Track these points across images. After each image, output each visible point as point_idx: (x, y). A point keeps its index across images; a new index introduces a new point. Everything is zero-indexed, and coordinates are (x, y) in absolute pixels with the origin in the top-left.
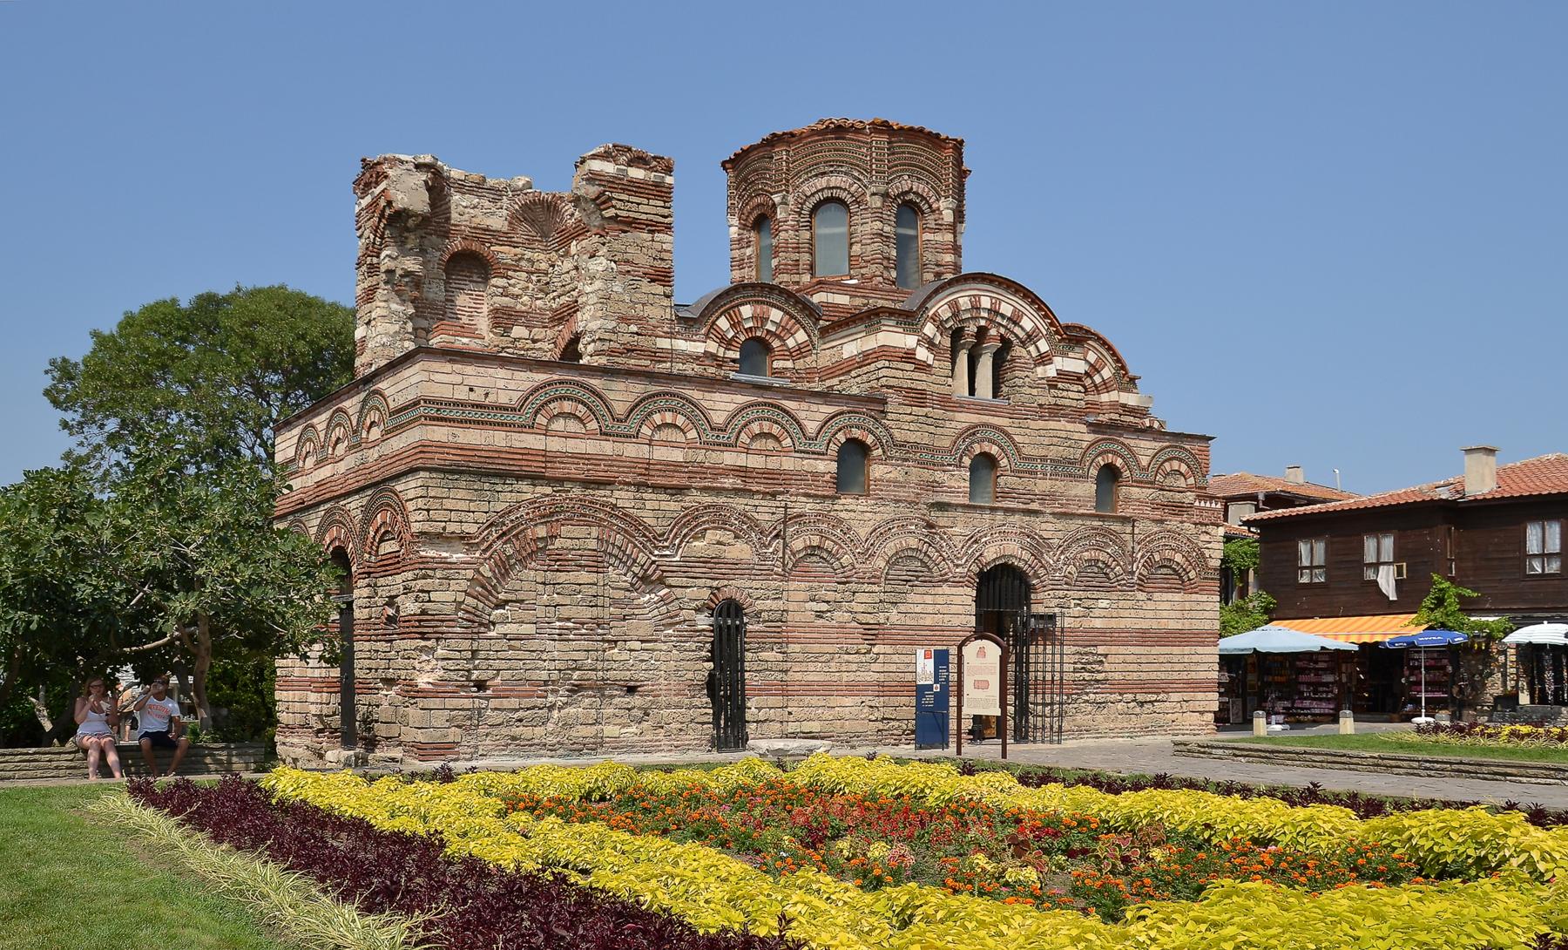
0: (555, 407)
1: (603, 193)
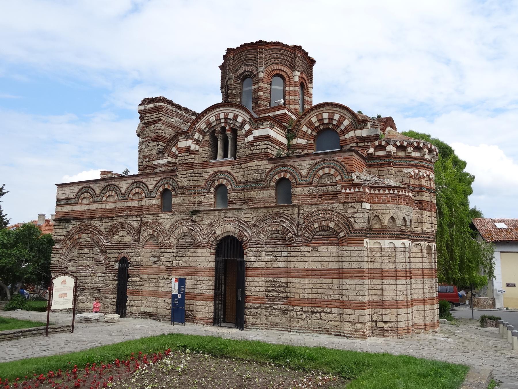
0: (83, 196)
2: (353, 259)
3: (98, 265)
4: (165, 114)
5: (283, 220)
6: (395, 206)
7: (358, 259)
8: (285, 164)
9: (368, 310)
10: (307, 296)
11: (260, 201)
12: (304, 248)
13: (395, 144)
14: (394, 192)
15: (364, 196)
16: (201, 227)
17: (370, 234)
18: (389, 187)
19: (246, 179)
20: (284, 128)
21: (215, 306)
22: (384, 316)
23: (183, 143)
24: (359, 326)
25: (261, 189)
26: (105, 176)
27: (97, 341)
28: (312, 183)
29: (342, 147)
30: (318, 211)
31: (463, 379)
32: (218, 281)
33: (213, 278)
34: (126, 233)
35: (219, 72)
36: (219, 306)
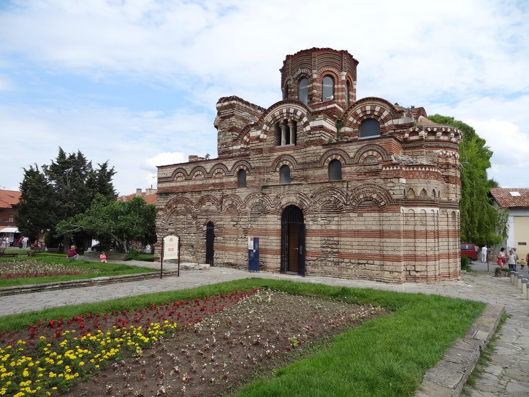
0: (177, 175)
2: (392, 223)
4: (237, 110)
5: (335, 192)
6: (426, 180)
7: (395, 223)
8: (337, 149)
9: (403, 262)
10: (354, 251)
11: (316, 178)
12: (351, 214)
13: (426, 130)
14: (425, 169)
15: (401, 173)
16: (270, 198)
17: (406, 203)
18: (422, 166)
19: (304, 161)
20: (334, 119)
21: (281, 258)
22: (416, 267)
23: (254, 133)
24: (396, 274)
25: (317, 169)
26: (192, 159)
27: (199, 283)
28: (358, 163)
29: (382, 133)
30: (363, 185)
31: (481, 311)
32: (283, 240)
33: (280, 238)
35: (280, 74)
36: (284, 259)
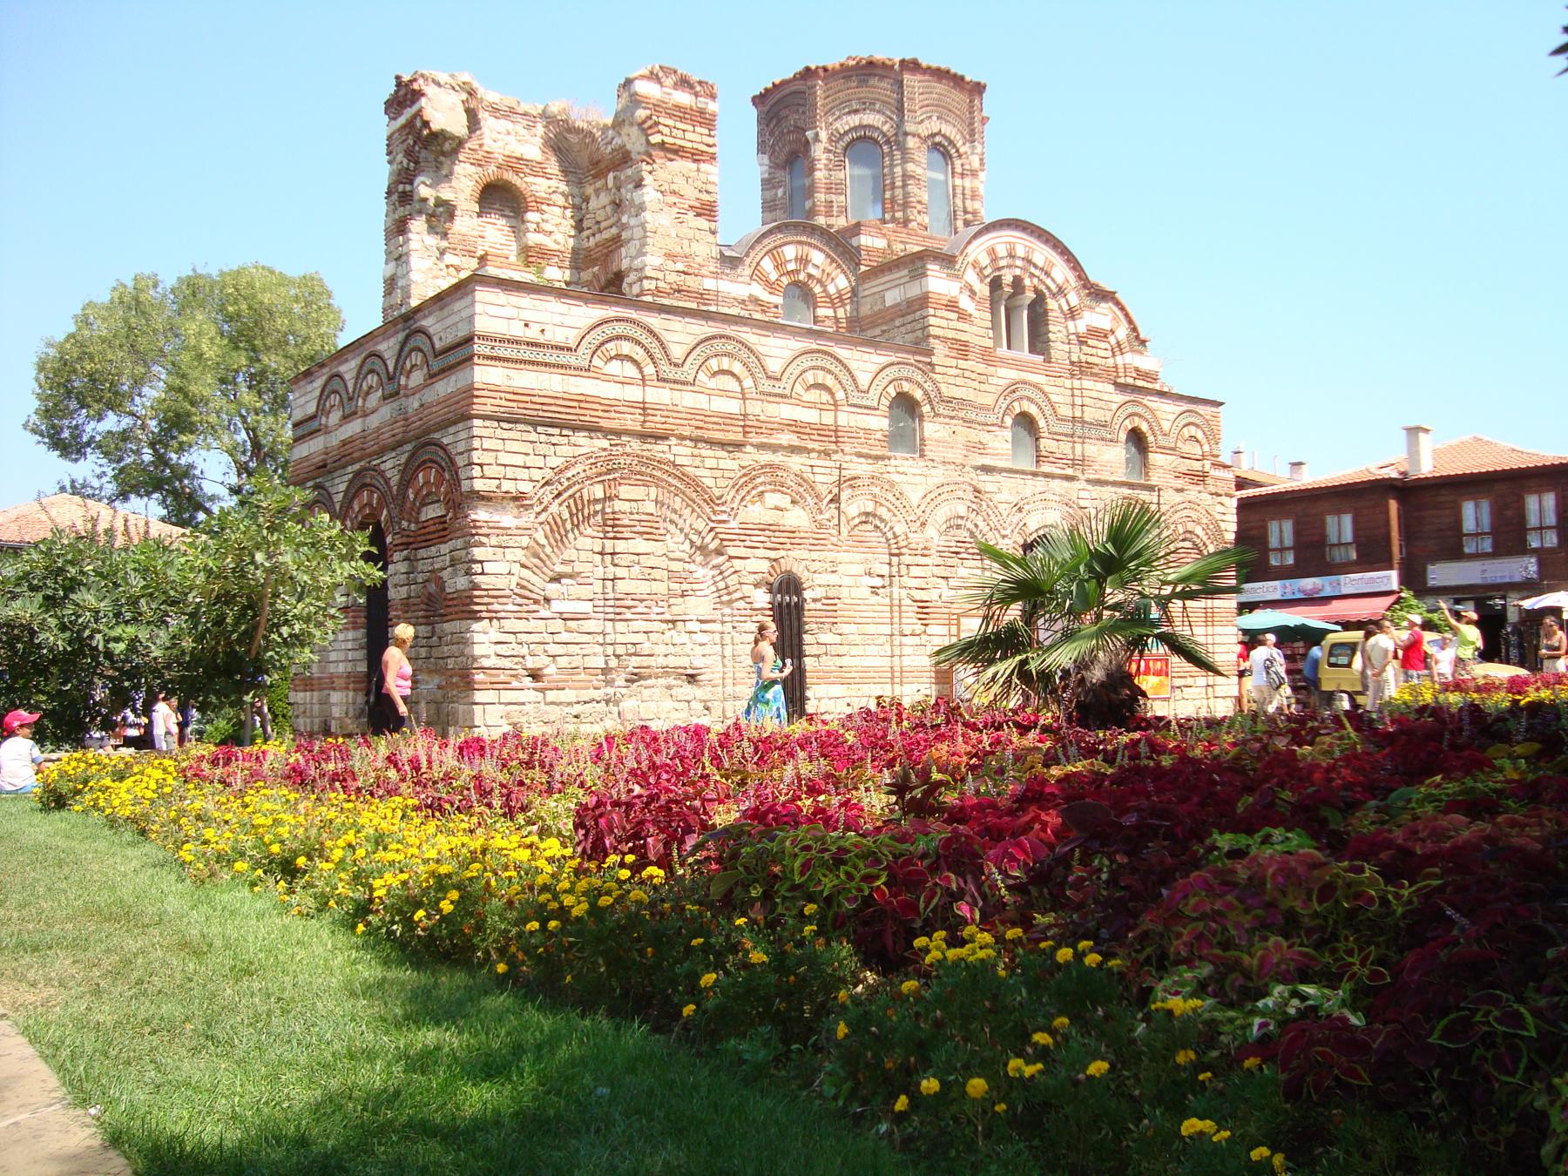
1: (650, 118)
3: (683, 596)
34: (789, 499)
